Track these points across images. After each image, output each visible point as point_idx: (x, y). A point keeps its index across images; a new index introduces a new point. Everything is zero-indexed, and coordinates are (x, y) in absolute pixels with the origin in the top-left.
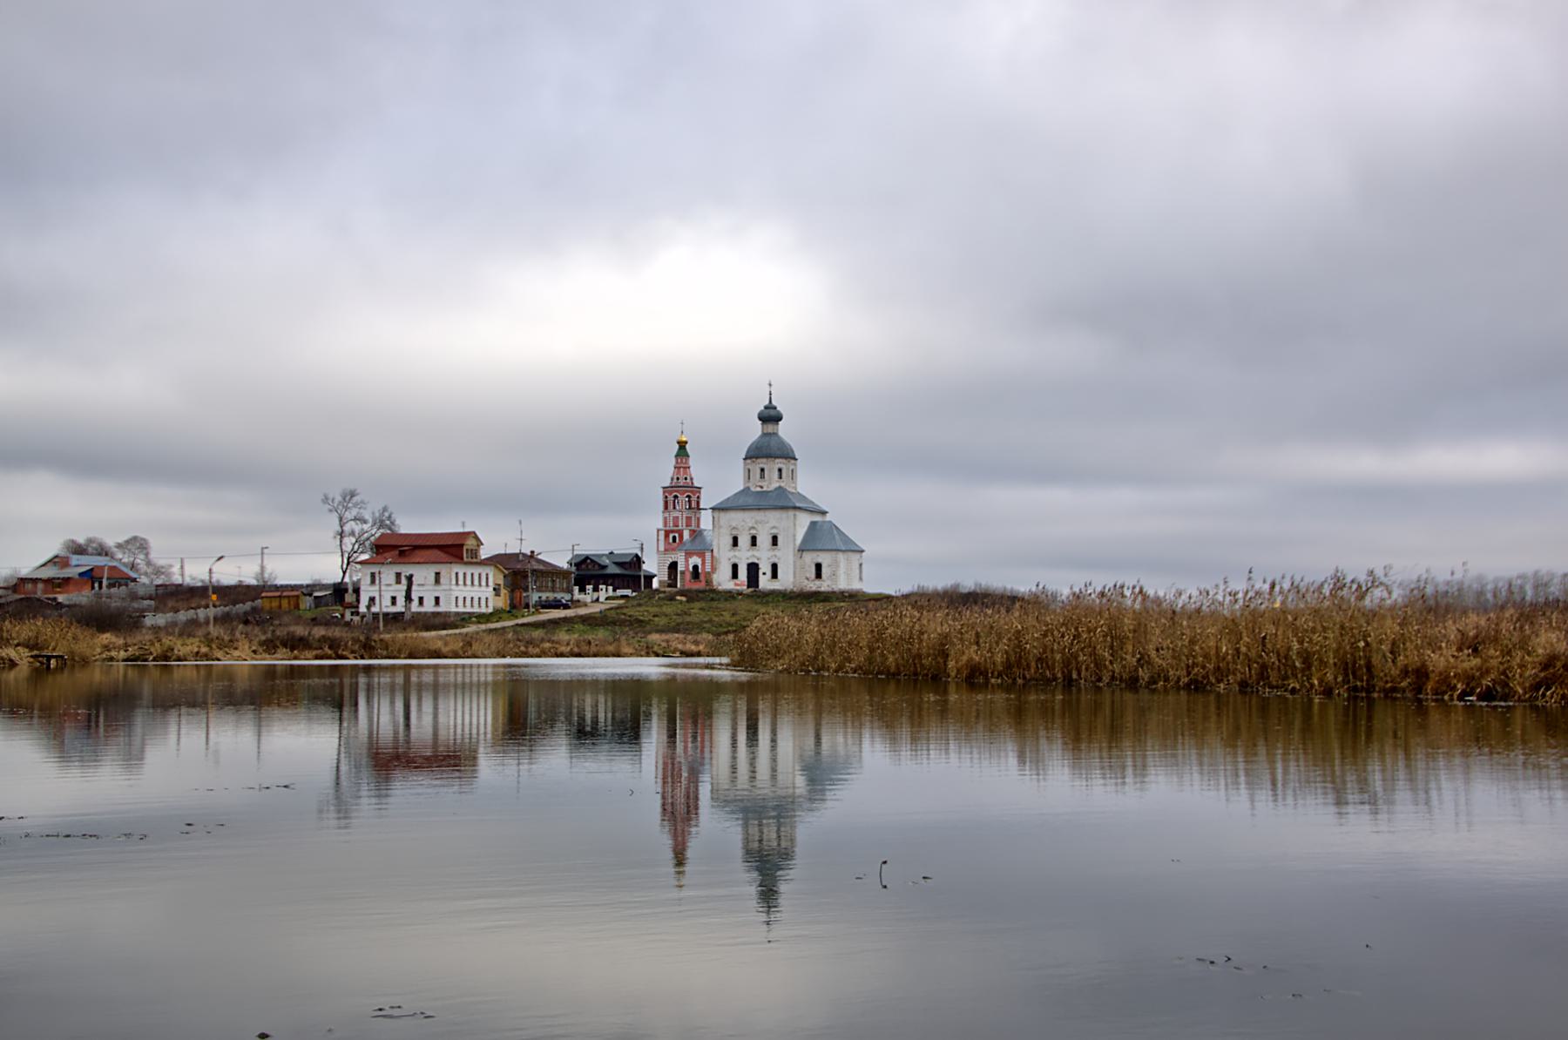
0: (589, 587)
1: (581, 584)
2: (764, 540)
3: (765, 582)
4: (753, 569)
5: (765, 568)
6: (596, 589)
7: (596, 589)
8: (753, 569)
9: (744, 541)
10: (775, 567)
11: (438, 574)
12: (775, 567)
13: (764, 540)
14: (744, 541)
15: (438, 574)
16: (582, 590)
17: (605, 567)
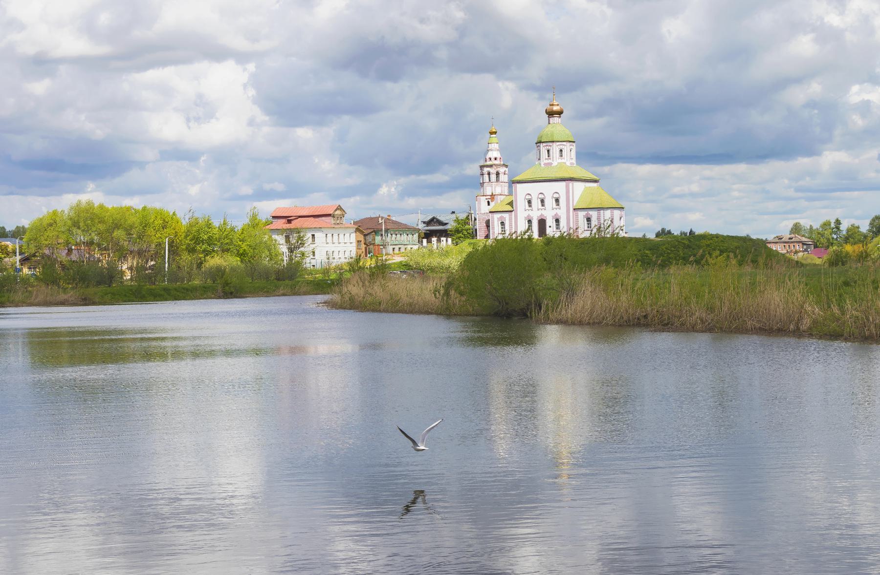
0: (434, 239)
1: (428, 235)
2: (550, 202)
3: (551, 231)
4: (542, 223)
5: (550, 222)
6: (439, 241)
7: (439, 241)
8: (542, 223)
9: (536, 203)
10: (557, 221)
11: (313, 235)
12: (557, 221)
13: (550, 202)
14: (536, 203)
15: (313, 235)
16: (429, 242)
17: (446, 224)
